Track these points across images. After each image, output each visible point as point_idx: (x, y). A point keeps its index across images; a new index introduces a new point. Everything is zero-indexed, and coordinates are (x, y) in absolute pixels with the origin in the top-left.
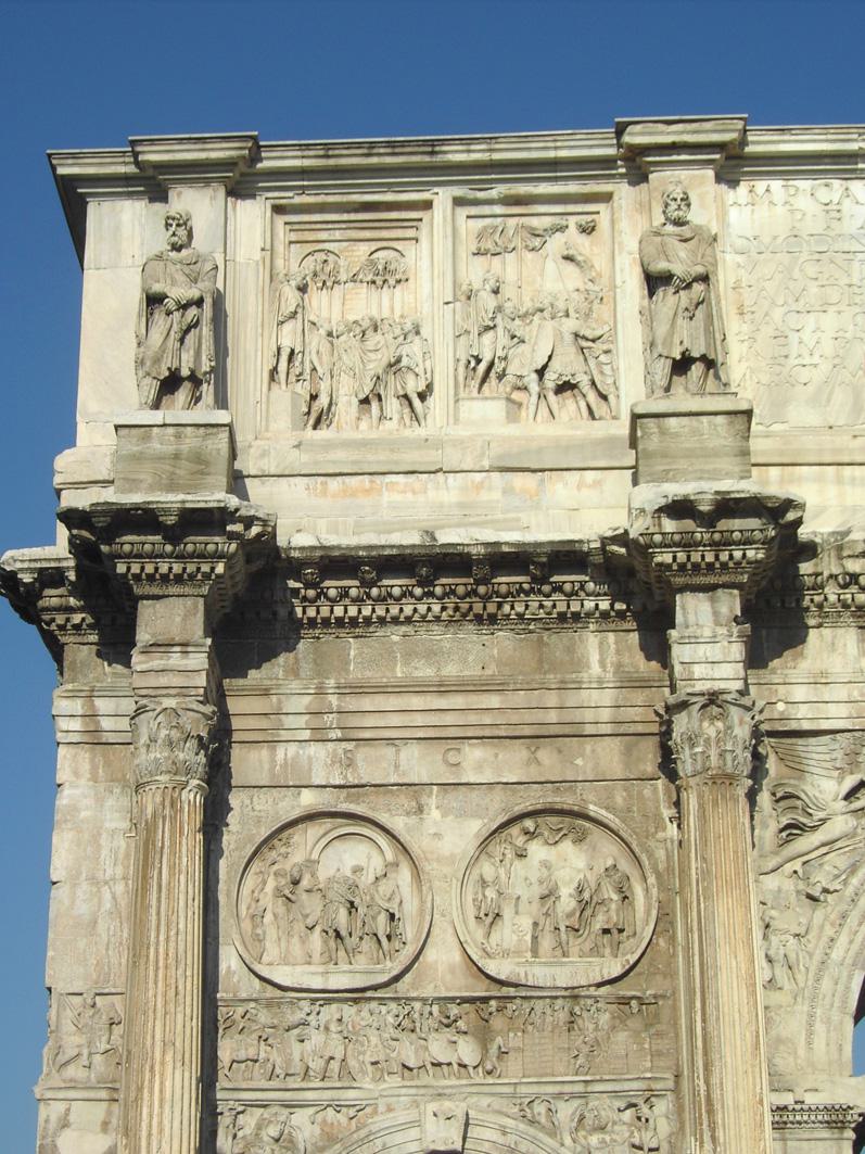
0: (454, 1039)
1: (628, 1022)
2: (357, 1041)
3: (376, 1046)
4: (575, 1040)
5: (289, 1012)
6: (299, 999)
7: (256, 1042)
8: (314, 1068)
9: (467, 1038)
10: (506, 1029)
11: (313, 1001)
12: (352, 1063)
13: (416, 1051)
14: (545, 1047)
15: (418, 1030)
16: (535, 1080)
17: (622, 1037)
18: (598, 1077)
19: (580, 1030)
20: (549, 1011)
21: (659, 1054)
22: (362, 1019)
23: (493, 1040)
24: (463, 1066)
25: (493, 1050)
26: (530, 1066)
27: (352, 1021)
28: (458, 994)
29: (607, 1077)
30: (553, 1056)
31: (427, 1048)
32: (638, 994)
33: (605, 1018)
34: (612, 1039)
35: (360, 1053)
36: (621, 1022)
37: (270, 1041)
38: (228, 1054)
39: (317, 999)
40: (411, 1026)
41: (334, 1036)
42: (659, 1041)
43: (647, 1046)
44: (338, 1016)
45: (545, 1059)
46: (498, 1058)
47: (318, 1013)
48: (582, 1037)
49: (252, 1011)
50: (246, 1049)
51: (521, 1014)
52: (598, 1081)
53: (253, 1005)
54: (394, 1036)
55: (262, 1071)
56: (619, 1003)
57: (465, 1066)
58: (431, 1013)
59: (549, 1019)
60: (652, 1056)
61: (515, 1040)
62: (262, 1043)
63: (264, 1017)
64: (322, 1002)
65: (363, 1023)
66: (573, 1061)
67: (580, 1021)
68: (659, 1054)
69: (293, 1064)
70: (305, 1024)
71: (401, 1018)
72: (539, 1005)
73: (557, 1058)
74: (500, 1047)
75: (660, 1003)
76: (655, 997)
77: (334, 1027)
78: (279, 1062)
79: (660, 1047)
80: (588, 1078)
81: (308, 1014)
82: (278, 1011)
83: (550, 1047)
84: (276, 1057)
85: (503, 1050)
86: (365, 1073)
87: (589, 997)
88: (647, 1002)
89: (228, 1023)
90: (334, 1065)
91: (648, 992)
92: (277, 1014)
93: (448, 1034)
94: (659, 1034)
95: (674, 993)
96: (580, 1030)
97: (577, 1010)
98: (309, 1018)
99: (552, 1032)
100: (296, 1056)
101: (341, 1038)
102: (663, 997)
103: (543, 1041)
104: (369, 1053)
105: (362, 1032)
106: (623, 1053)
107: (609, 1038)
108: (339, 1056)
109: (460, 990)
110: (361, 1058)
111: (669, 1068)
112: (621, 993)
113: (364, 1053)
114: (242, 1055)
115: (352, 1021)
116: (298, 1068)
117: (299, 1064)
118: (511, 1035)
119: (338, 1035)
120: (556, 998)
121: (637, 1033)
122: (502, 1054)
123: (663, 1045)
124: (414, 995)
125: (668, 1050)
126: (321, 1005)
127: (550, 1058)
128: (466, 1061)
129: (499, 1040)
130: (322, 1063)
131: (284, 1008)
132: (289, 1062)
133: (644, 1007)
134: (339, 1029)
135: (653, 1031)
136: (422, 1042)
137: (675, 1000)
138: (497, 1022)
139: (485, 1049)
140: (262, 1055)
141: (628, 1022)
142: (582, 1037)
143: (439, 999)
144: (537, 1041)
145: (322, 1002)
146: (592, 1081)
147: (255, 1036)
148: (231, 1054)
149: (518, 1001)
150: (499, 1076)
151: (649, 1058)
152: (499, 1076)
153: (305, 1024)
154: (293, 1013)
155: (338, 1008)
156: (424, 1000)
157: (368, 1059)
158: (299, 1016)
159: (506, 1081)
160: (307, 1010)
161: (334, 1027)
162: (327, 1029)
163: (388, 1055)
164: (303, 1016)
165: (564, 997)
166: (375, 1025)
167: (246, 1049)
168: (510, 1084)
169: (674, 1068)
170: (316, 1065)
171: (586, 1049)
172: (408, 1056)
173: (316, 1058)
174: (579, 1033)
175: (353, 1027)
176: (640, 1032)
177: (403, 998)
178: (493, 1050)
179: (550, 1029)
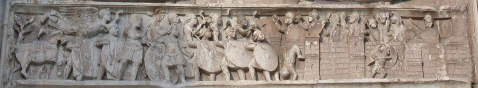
0: (251, 46)
1: (423, 35)
2: (155, 47)
3: (174, 51)
4: (371, 49)
5: (90, 20)
6: (99, 8)
7: (55, 46)
8: (111, 72)
9: (265, 46)
10: (302, 38)
11: (113, 12)
12: (150, 67)
13: (214, 58)
14: (342, 55)
15: (216, 37)
16: (332, 81)
17: (415, 47)
18: (396, 80)
19: (375, 40)
20: (343, 23)
21: (454, 62)
22: (161, 28)
23: (288, 49)
24: (259, 71)
25: (289, 58)
26: (326, 72)
27: (152, 31)
28: (255, 5)
29: (405, 80)
30: (349, 64)
31: (223, 55)
32: (433, 9)
33: (398, 30)
34: (407, 49)
35: (157, 58)
36: (416, 35)
37: (69, 45)
38: (26, 54)
39: (118, 8)
40: (208, 34)
41: (133, 41)
42: (454, 51)
43: (441, 56)
44: (137, 24)
45: (341, 66)
46: (295, 64)
47: (118, 22)
48: (377, 47)
49: (53, 18)
50: (45, 52)
51: (316, 25)
52: (395, 83)
53: (54, 12)
54: (192, 43)
55: (59, 73)
56: (413, 18)
57: (262, 71)
58: (229, 24)
59: (344, 31)
60: (448, 64)
61: (310, 48)
62: (61, 48)
63: (64, 24)
64: (121, 11)
65: (162, 32)
66: (368, 68)
67: (376, 33)
68: (454, 62)
69: (91, 68)
70: (105, 32)
71: (199, 26)
72: (335, 18)
73: (352, 65)
74: (296, 56)
75: (454, 17)
76: (449, 11)
77: (133, 34)
78: (77, 63)
79: (456, 57)
80: (386, 80)
81: (108, 22)
82: (78, 19)
83: (347, 55)
84: (73, 59)
85: (299, 56)
86: (162, 77)
87: (384, 10)
88: (441, 17)
89: (28, 29)
90: (133, 70)
91: (442, 8)
92: (77, 21)
93: (244, 43)
94: (453, 45)
95: (467, 9)
96: (375, 40)
97: (372, 22)
98: (108, 26)
99: (348, 42)
100: (95, 61)
101: (139, 44)
102: (457, 11)
103: (339, 50)
104: (166, 58)
105: (161, 40)
106: (419, 62)
107: (404, 49)
108: (137, 59)
109: (258, 2)
110: (159, 63)
111: (465, 76)
112: (416, 7)
113: (162, 59)
114: (40, 57)
115: (152, 31)
116: (94, 71)
117: (96, 68)
118: (308, 43)
119: (137, 42)
120: (351, 10)
121: (432, 46)
122: (298, 61)
123: (460, 54)
124: (213, 5)
125: (463, 60)
126: (120, 15)
127: (346, 66)
128: (263, 66)
129: (295, 48)
130: (120, 66)
131: (84, 16)
132: (87, 66)
133: (438, 22)
134: (138, 35)
135: (447, 42)
136: (219, 49)
137: (468, 15)
138: (293, 33)
139: (280, 59)
140: (60, 59)
141: (423, 35)
142: (377, 47)
143: (238, 10)
144: (333, 50)
145: (121, 11)
146: (389, 83)
147: (54, 40)
148: (29, 55)
149: (314, 14)
150: (297, 78)
151: (444, 67)
152: (297, 78)
153: (105, 32)
154: (93, 21)
155: (137, 17)
156: (222, 10)
157: (166, 62)
158: (99, 23)
159: (304, 82)
160: (107, 17)
161: (133, 34)
162: (126, 35)
163: (185, 61)
164: (103, 22)
165: (359, 10)
166: (174, 32)
167: (45, 52)
168: (306, 85)
169: (471, 75)
170: (113, 68)
171: (382, 57)
172: (205, 60)
173: (114, 62)
174: (374, 42)
175: (152, 36)
176: (435, 44)
177: (202, 8)
178: (289, 58)
179: (345, 40)
